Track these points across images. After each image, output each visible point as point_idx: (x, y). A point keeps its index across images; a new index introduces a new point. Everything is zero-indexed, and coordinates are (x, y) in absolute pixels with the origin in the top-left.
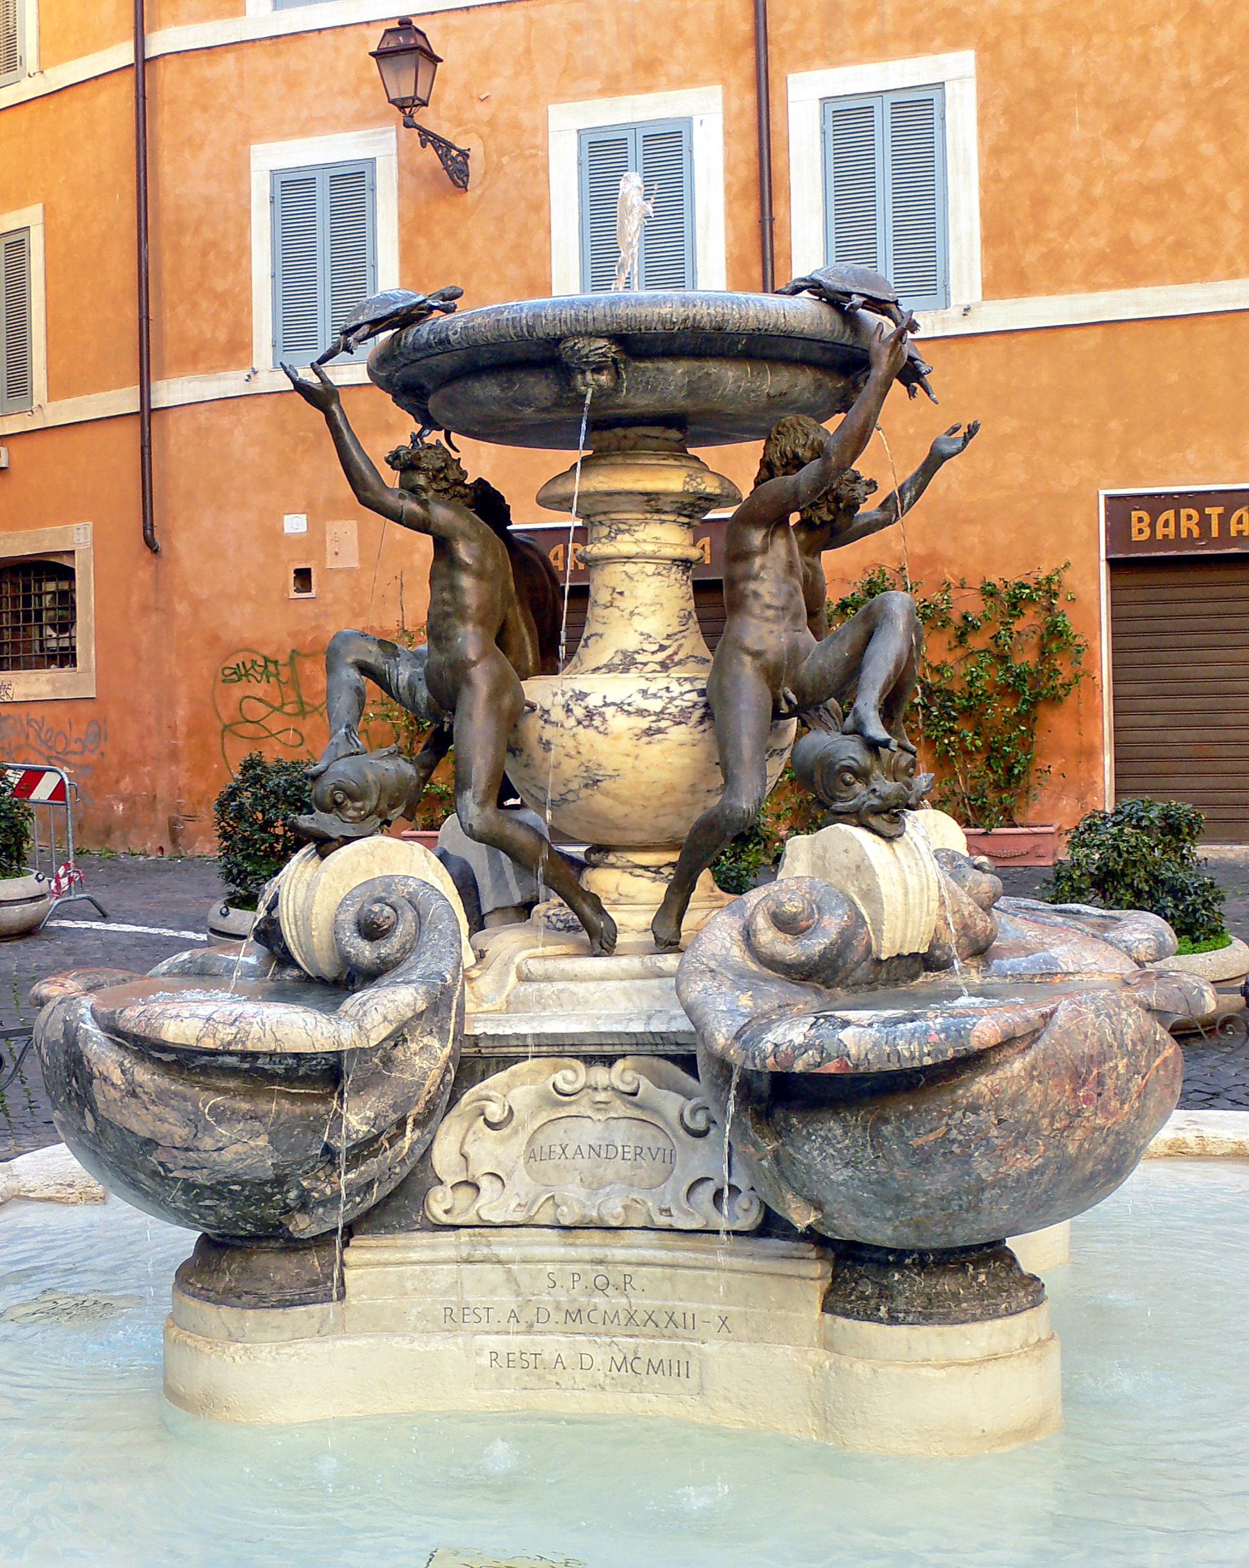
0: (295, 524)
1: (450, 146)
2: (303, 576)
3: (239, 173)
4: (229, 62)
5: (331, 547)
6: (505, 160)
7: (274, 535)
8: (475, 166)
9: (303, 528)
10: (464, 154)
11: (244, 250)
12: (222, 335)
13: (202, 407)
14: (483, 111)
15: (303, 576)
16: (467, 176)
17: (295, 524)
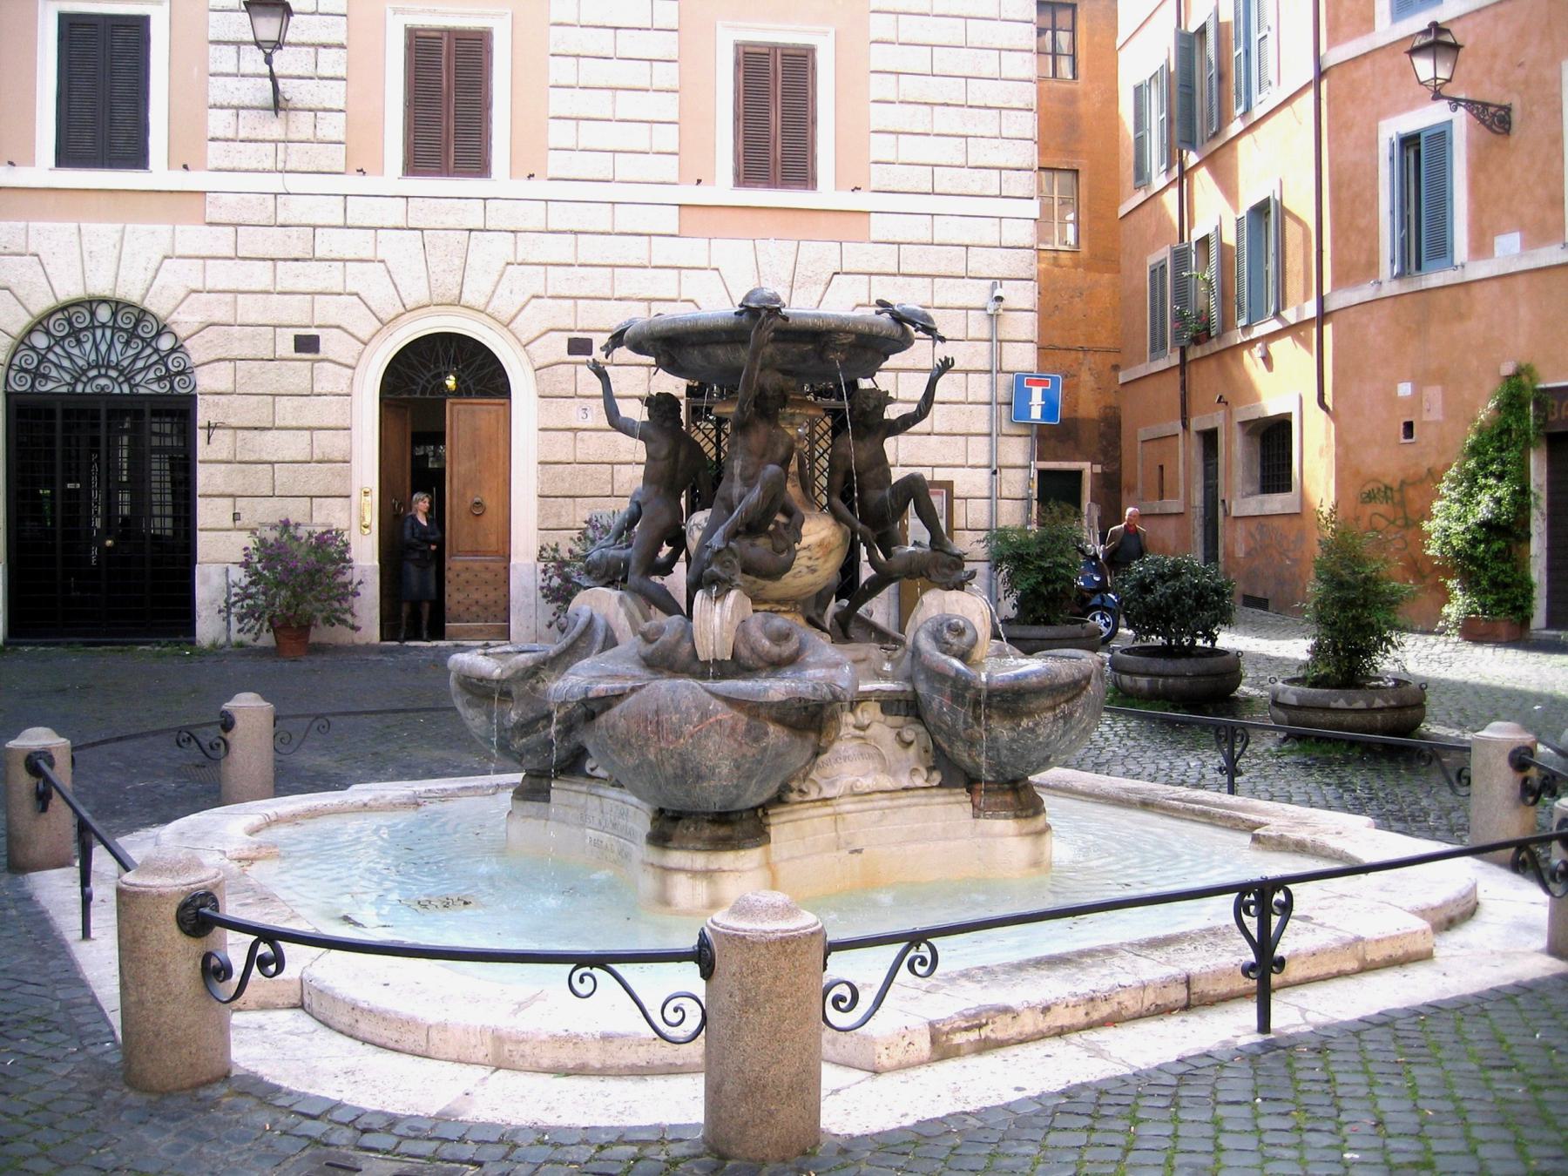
0: (1405, 389)
1: (1486, 105)
2: (1409, 428)
3: (1375, 142)
4: (1367, 66)
5: (1426, 405)
6: (1535, 108)
7: (1391, 398)
8: (1516, 116)
9: (1409, 392)
10: (1507, 109)
11: (1376, 196)
12: (1363, 259)
13: (1351, 310)
14: (1520, 74)
15: (1409, 428)
16: (1510, 123)
17: (1405, 389)
